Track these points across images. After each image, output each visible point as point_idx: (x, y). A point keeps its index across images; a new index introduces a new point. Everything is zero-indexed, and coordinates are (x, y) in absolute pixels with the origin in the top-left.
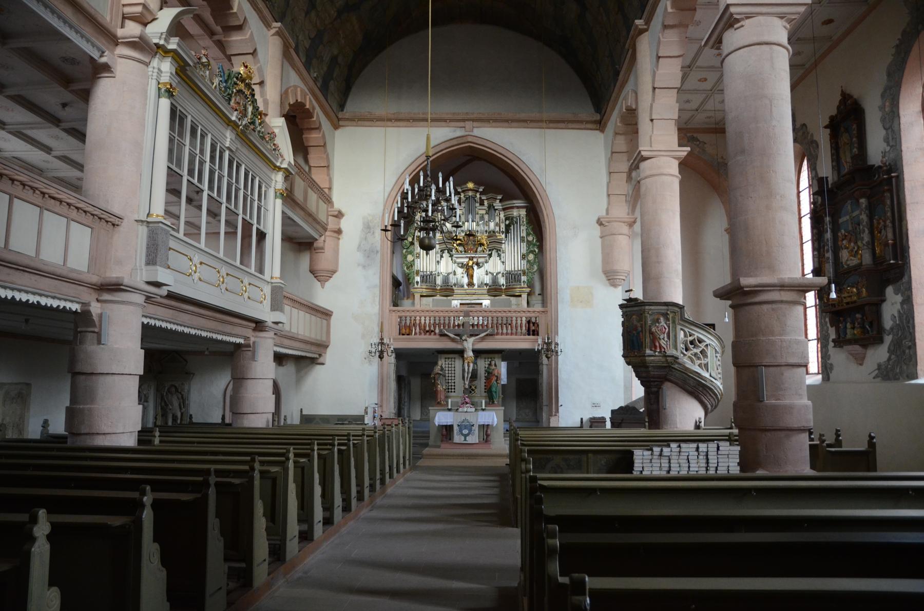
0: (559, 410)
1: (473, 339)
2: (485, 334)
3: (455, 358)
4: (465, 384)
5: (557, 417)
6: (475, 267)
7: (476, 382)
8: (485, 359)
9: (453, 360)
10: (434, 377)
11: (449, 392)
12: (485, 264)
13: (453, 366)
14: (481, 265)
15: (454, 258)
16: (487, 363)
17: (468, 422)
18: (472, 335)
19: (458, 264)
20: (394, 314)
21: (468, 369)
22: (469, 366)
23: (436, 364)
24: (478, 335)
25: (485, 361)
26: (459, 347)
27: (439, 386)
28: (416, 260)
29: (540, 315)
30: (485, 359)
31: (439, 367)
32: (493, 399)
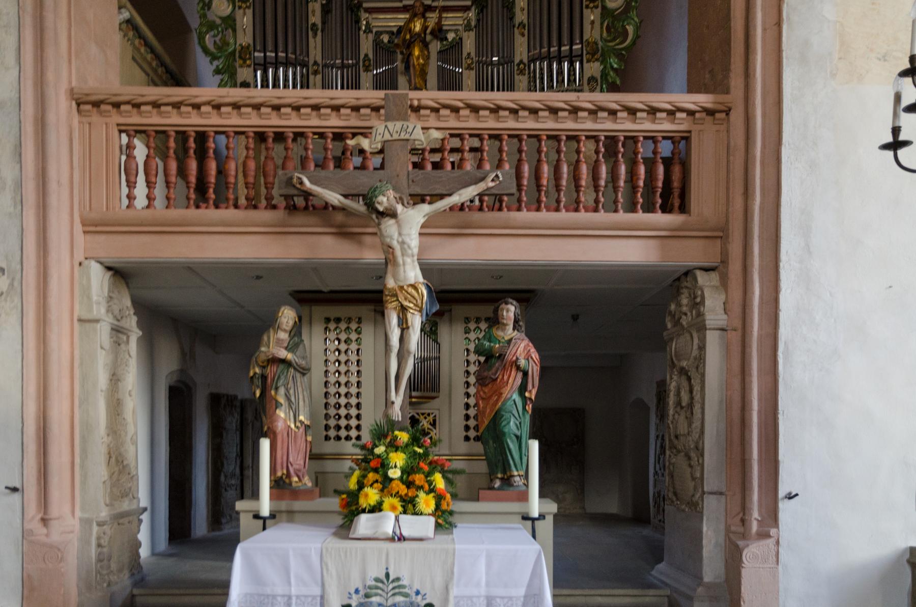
0: (782, 516)
1: (426, 208)
2: (470, 192)
3: (360, 321)
4: (389, 403)
5: (770, 542)
6: (435, 46)
7: (435, 403)
8: (467, 320)
9: (354, 326)
10: (264, 377)
11: (327, 438)
12: (465, 35)
13: (354, 347)
14: (451, 36)
15: (364, 16)
16: (472, 336)
17: (399, 589)
18: (419, 199)
19: (379, 34)
20: (95, 118)
21: (402, 339)
22: (404, 326)
23: (270, 322)
24: (442, 197)
25: (467, 331)
26: (371, 256)
27: (281, 413)
28: (239, 13)
29: (695, 128)
30: (467, 320)
31: (283, 336)
32: (506, 468)
